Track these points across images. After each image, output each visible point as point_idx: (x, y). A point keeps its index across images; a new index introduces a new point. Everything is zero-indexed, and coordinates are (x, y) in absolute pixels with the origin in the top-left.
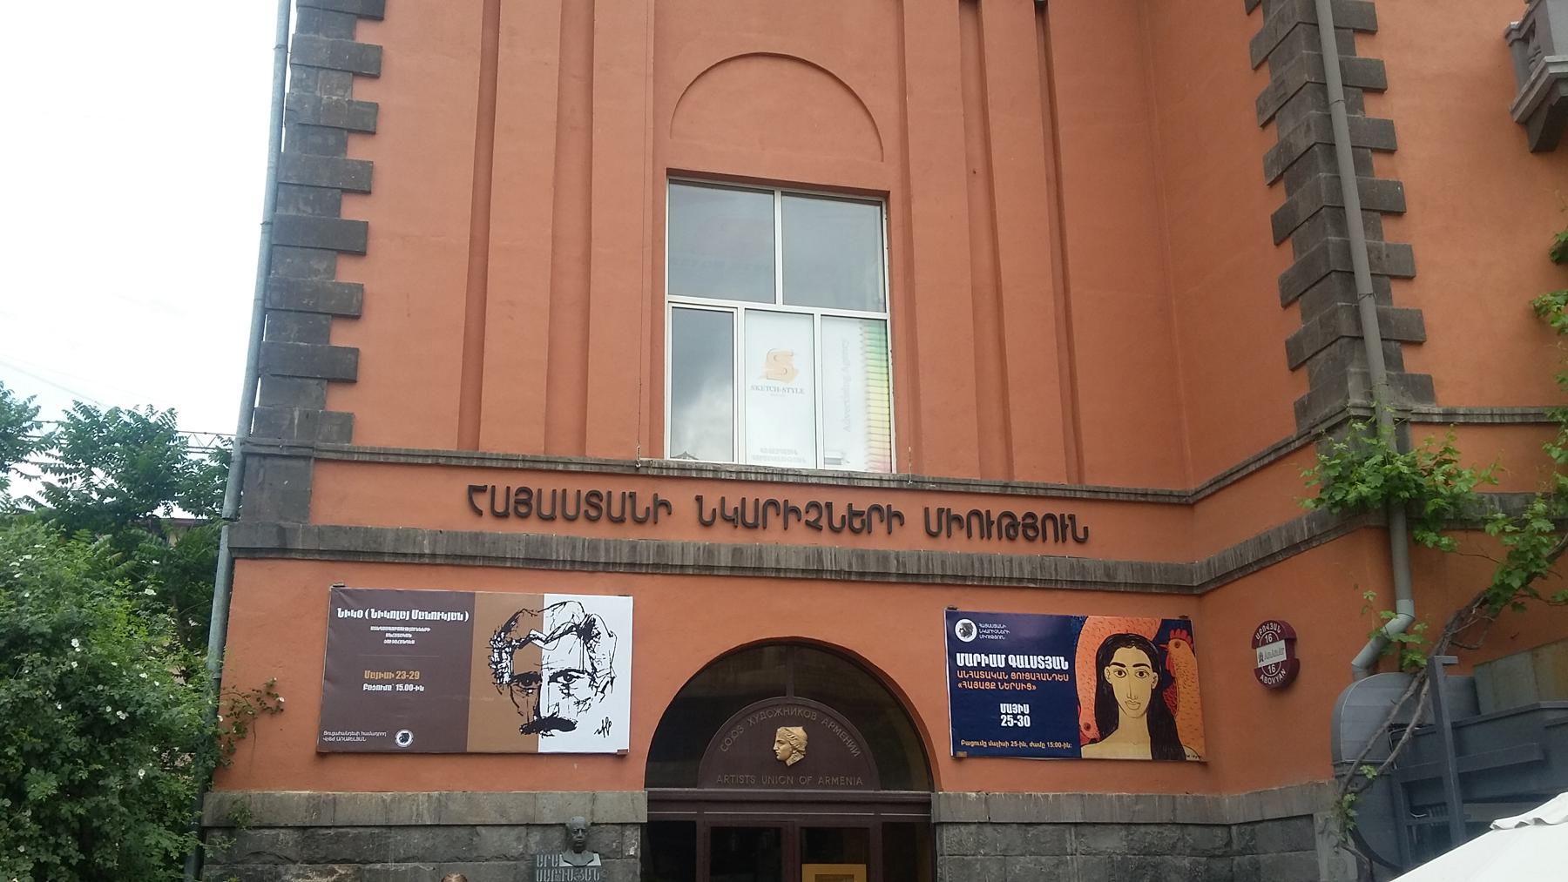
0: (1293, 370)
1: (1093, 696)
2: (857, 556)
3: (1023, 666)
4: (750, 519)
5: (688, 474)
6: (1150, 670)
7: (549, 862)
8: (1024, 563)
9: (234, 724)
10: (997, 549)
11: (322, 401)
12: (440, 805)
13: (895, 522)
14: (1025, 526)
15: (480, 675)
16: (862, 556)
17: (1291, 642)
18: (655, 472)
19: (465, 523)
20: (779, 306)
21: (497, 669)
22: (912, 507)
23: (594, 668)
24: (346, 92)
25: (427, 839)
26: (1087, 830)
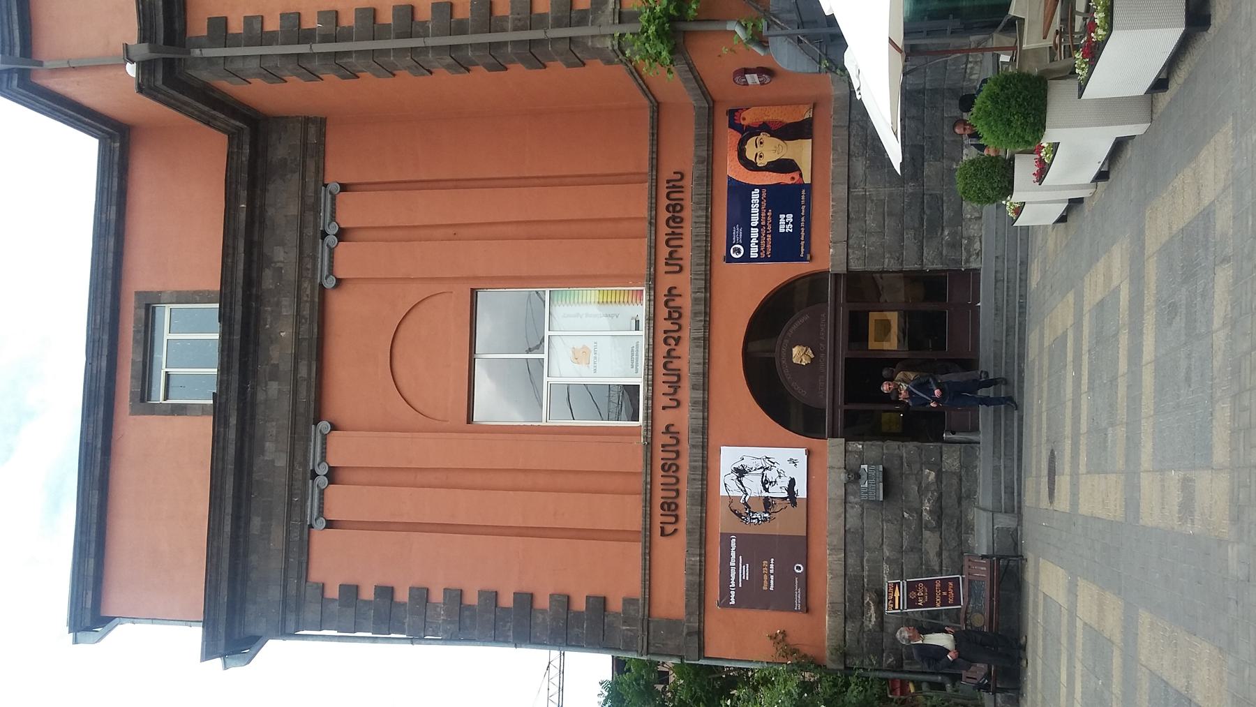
0: (584, 64)
1: (775, 174)
2: (695, 316)
3: (758, 217)
4: (675, 379)
5: (649, 415)
6: (759, 137)
7: (865, 493)
8: (697, 214)
9: (791, 655)
10: (688, 230)
11: (616, 614)
12: (834, 549)
13: (674, 292)
14: (674, 211)
15: (765, 529)
16: (695, 314)
17: (747, 71)
18: (649, 433)
19: (682, 538)
20: (545, 356)
21: (762, 521)
22: (665, 282)
23: (761, 468)
24: (438, 607)
25: (852, 555)
26: (852, 181)
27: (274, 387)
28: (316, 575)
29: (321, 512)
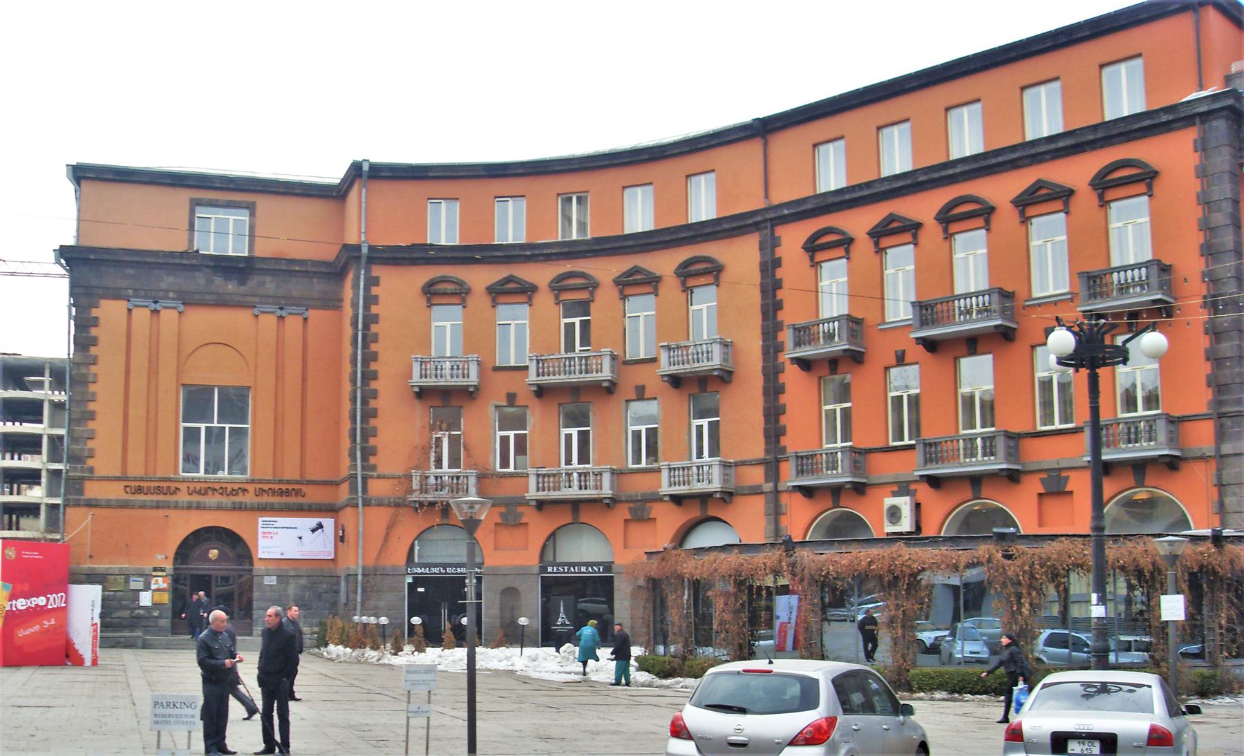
16: (234, 503)
22: (250, 488)
27: (202, 281)
28: (103, 302)
29: (136, 306)
